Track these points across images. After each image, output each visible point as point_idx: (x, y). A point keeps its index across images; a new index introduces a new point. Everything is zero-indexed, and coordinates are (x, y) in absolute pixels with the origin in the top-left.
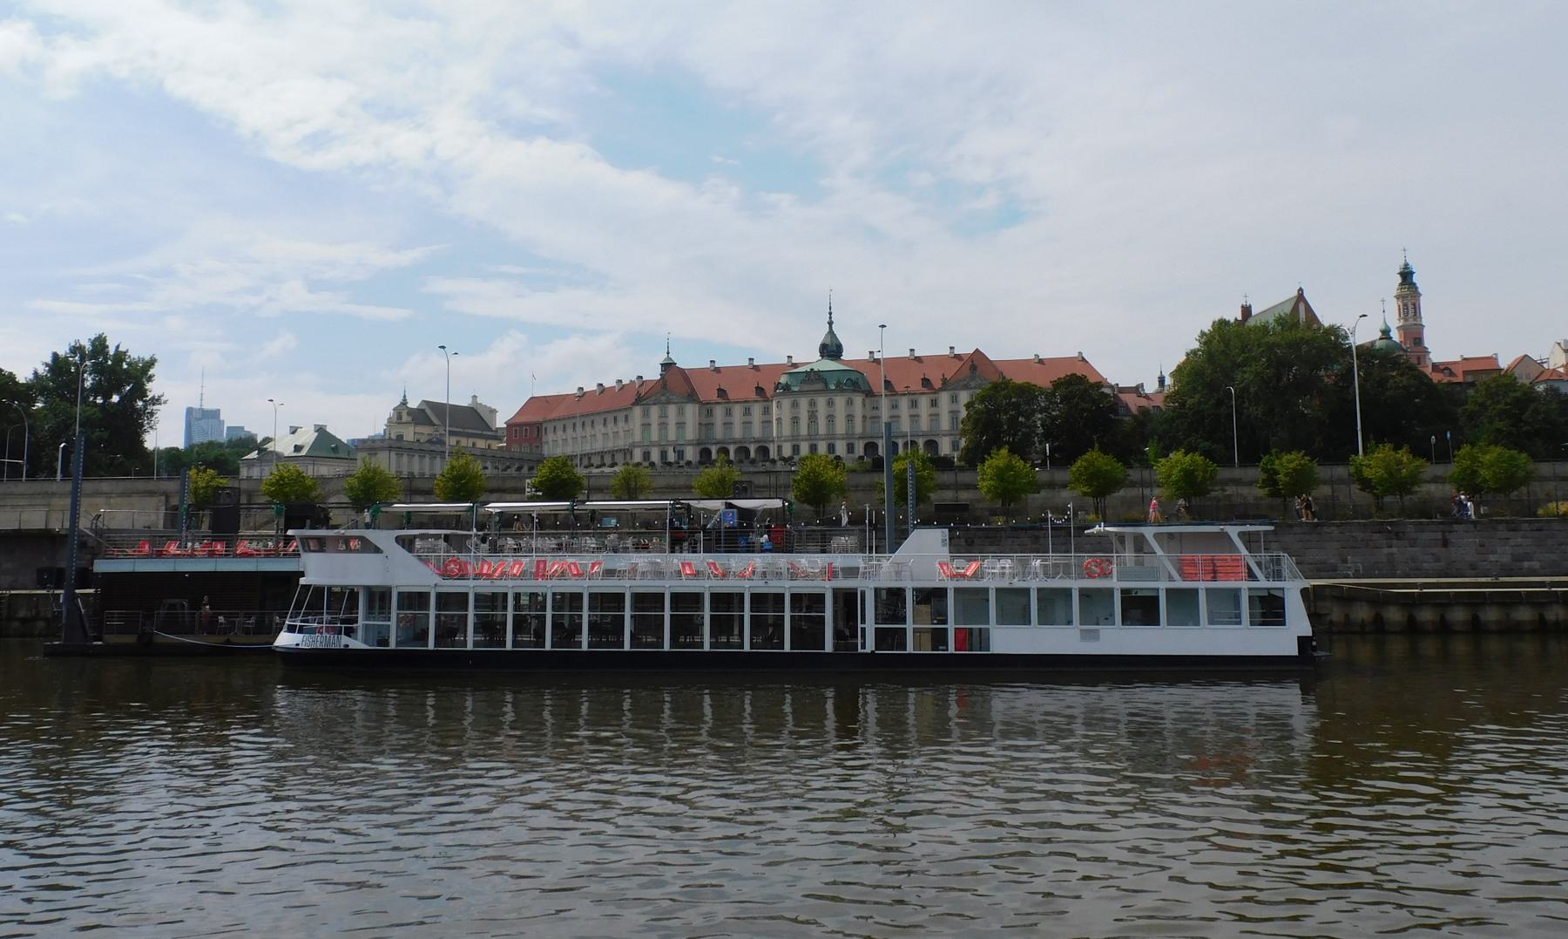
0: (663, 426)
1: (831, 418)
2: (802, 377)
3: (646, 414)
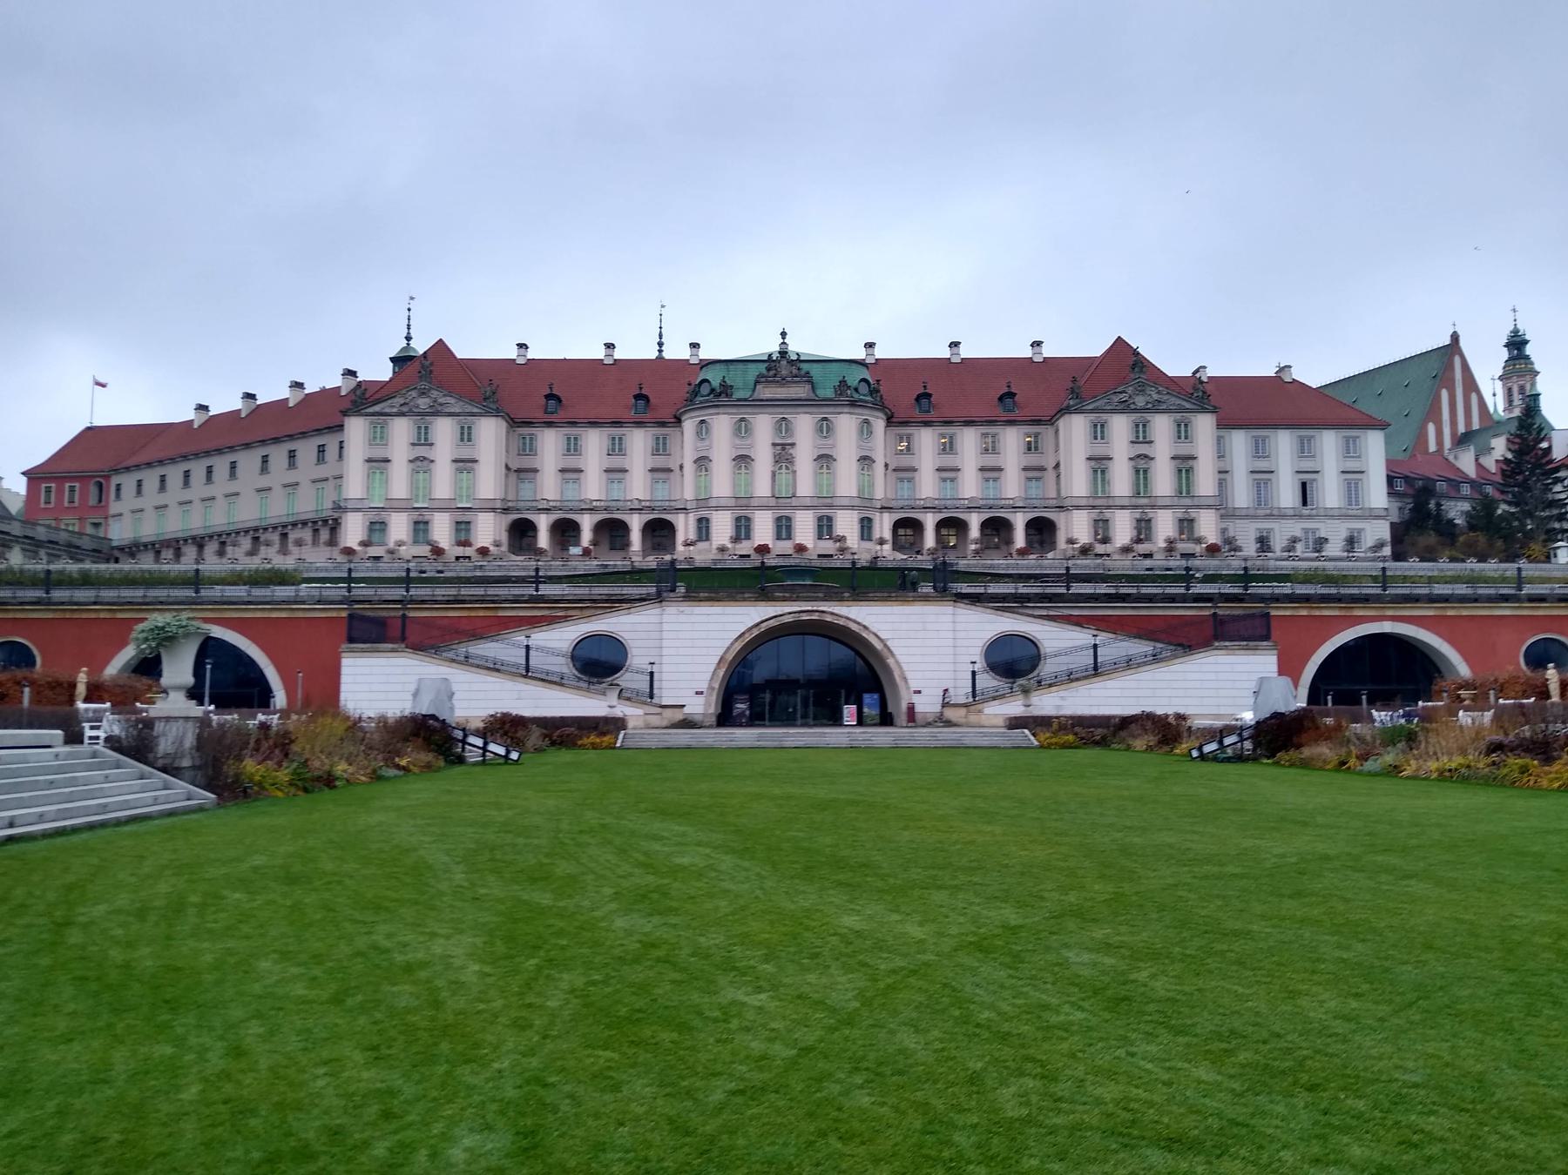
1: (825, 460)
2: (753, 371)
3: (378, 436)
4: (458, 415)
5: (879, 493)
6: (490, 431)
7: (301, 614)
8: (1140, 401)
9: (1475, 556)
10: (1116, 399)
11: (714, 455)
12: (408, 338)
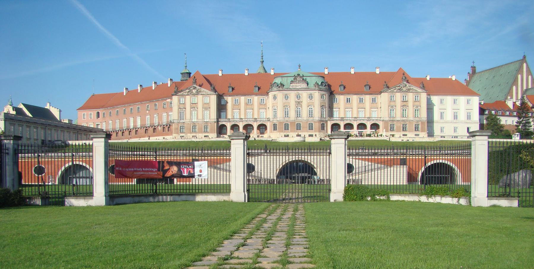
8: (404, 89)
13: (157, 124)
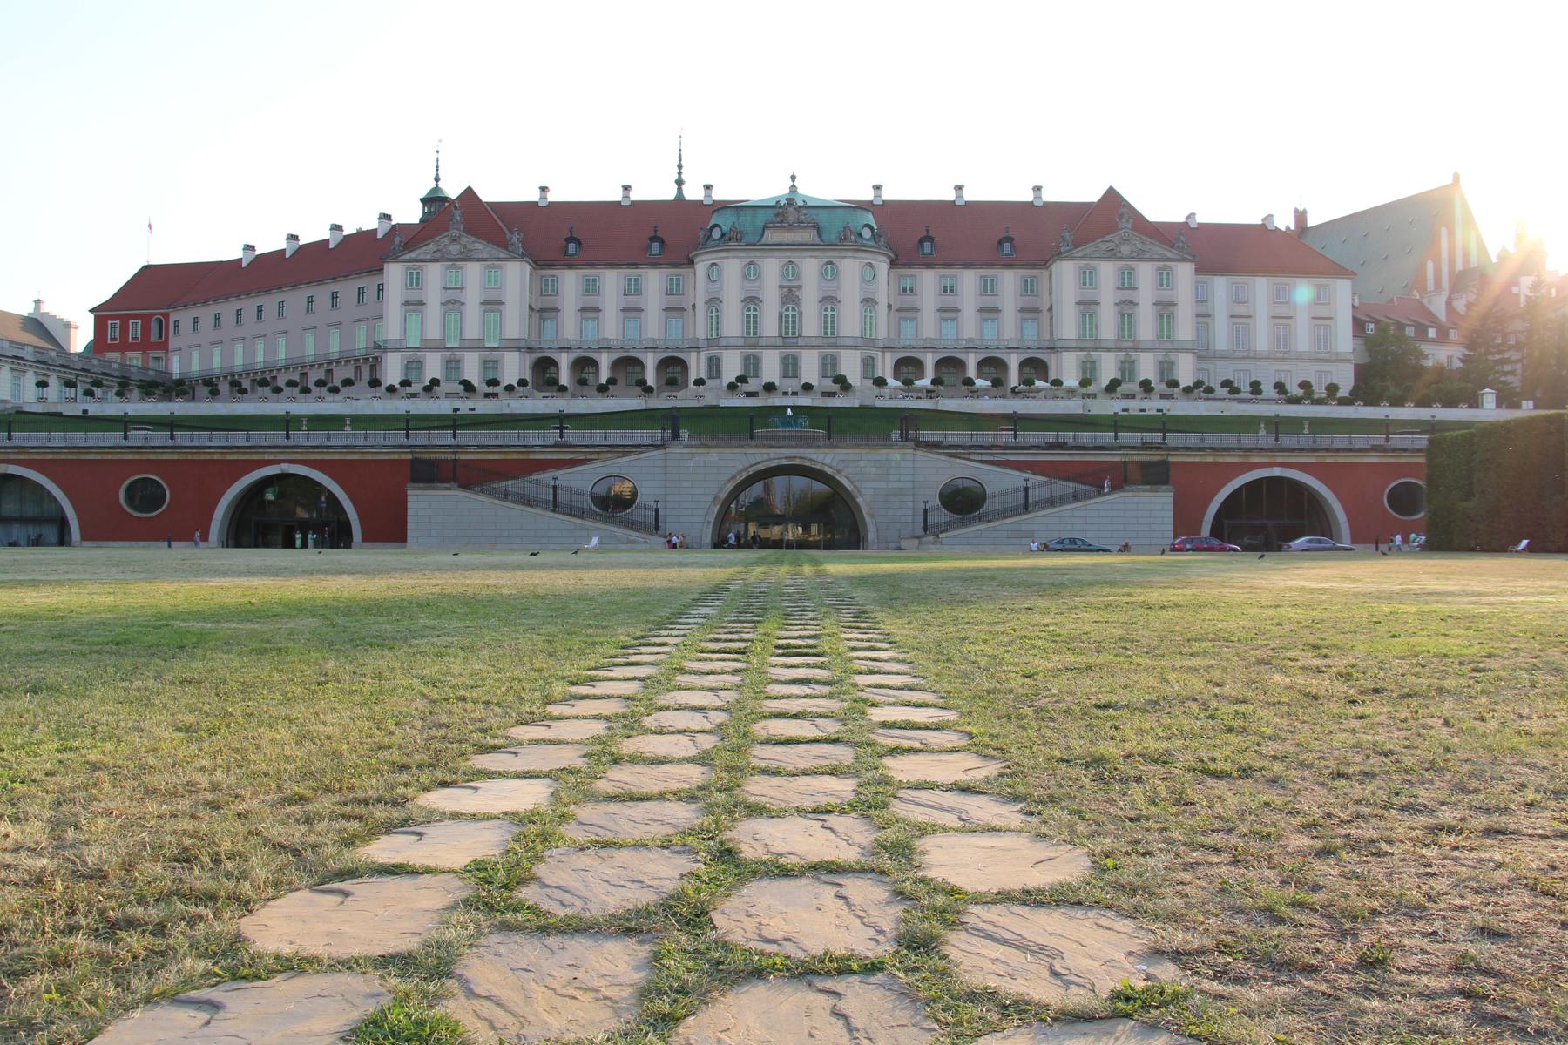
0: (453, 305)
1: (829, 301)
2: (762, 218)
4: (485, 260)
5: (882, 333)
6: (516, 276)
7: (369, 457)
8: (1126, 250)
9: (1440, 401)
10: (1103, 247)
11: (725, 297)
12: (437, 179)
13: (336, 356)
